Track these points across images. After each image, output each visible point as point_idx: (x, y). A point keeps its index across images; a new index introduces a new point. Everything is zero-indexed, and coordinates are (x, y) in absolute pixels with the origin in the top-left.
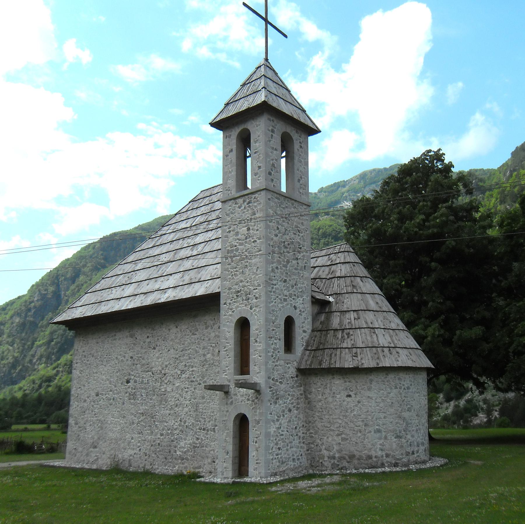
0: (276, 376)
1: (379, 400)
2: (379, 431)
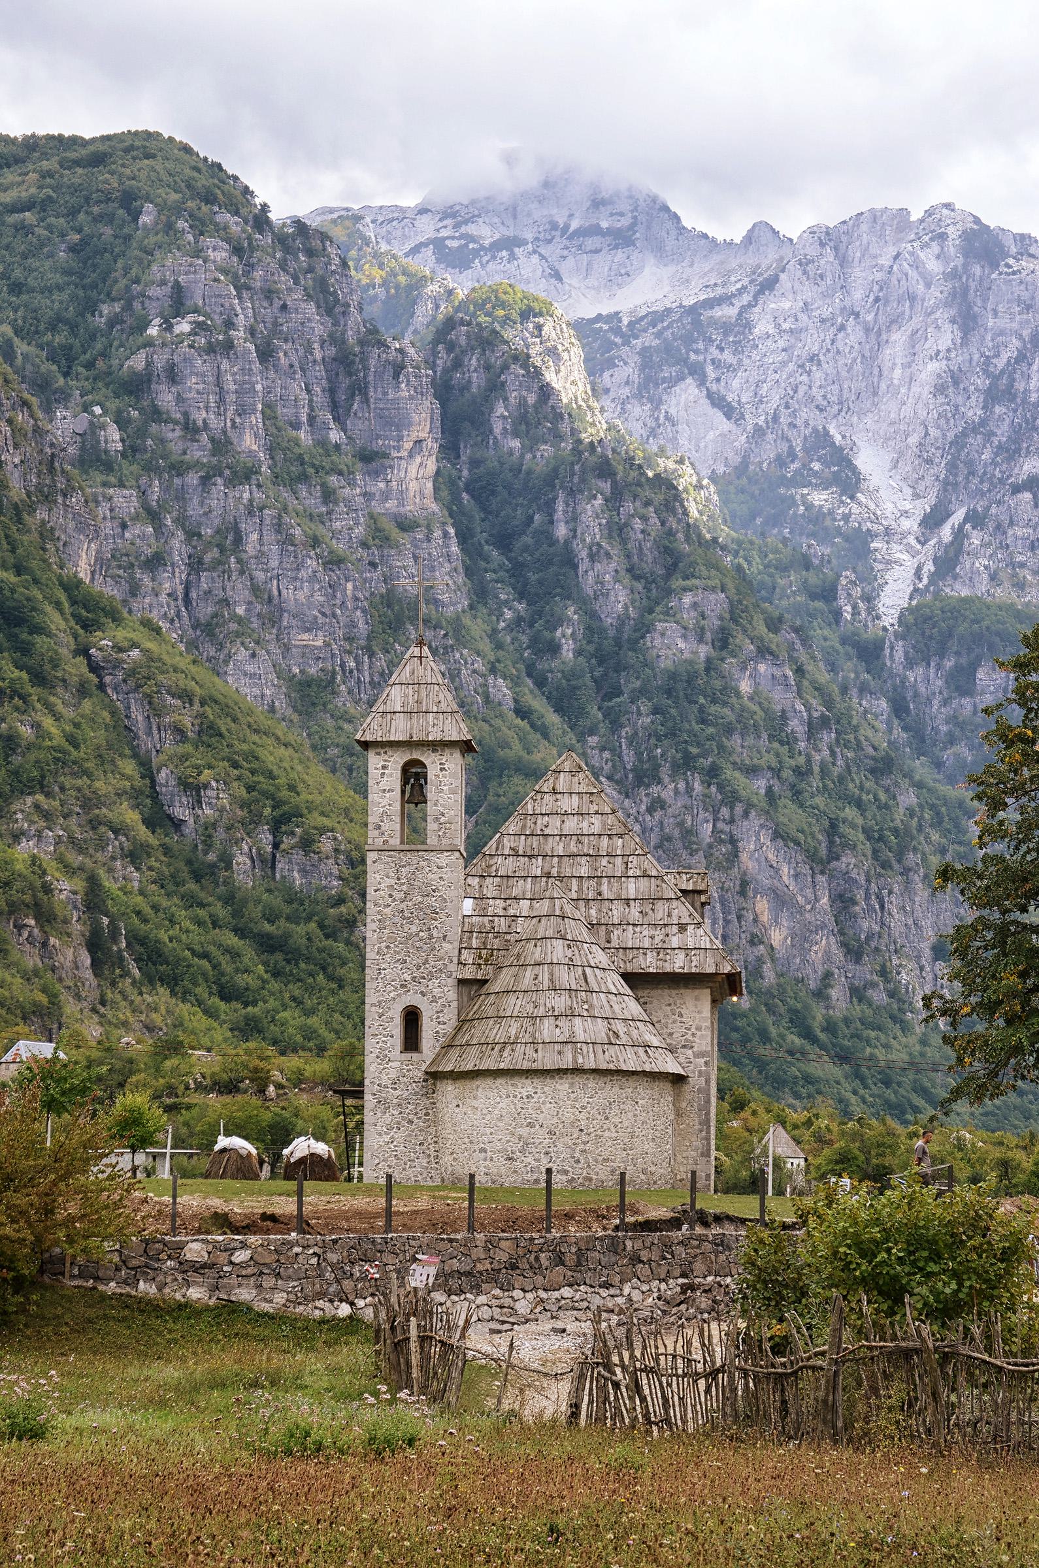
0: (385, 1080)
1: (485, 1111)
2: (486, 1152)
